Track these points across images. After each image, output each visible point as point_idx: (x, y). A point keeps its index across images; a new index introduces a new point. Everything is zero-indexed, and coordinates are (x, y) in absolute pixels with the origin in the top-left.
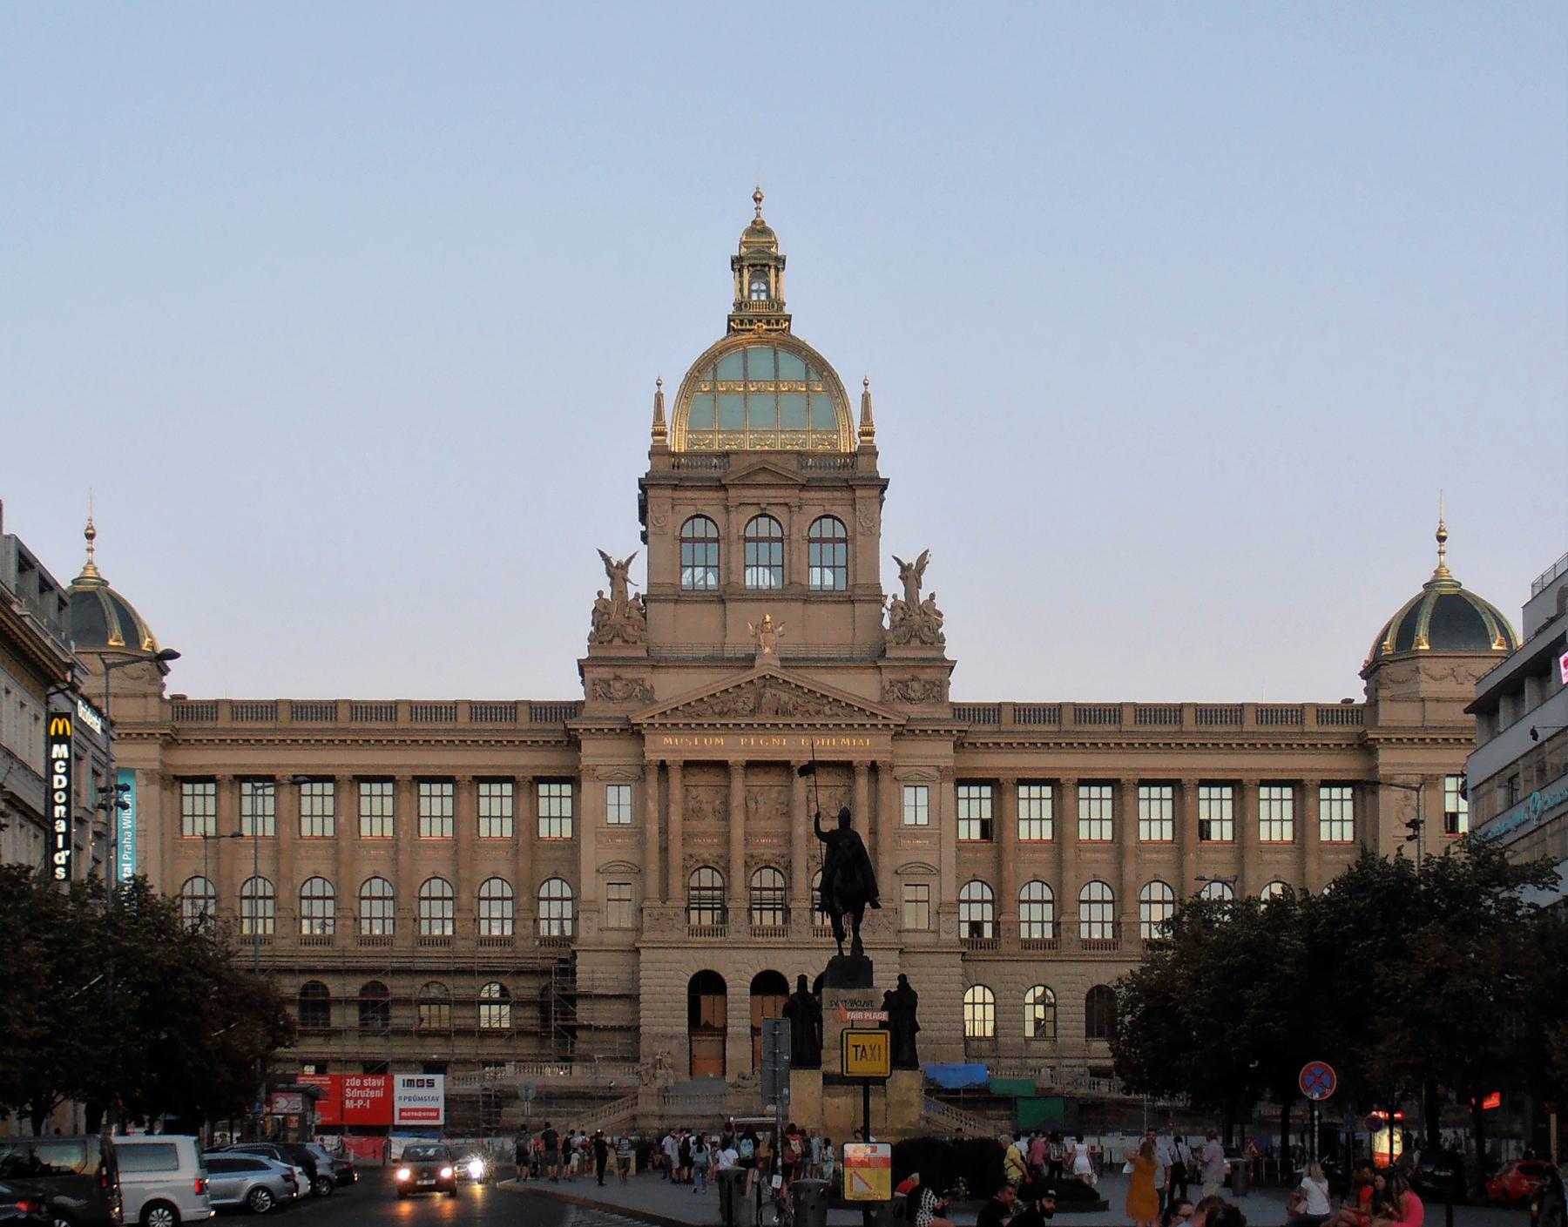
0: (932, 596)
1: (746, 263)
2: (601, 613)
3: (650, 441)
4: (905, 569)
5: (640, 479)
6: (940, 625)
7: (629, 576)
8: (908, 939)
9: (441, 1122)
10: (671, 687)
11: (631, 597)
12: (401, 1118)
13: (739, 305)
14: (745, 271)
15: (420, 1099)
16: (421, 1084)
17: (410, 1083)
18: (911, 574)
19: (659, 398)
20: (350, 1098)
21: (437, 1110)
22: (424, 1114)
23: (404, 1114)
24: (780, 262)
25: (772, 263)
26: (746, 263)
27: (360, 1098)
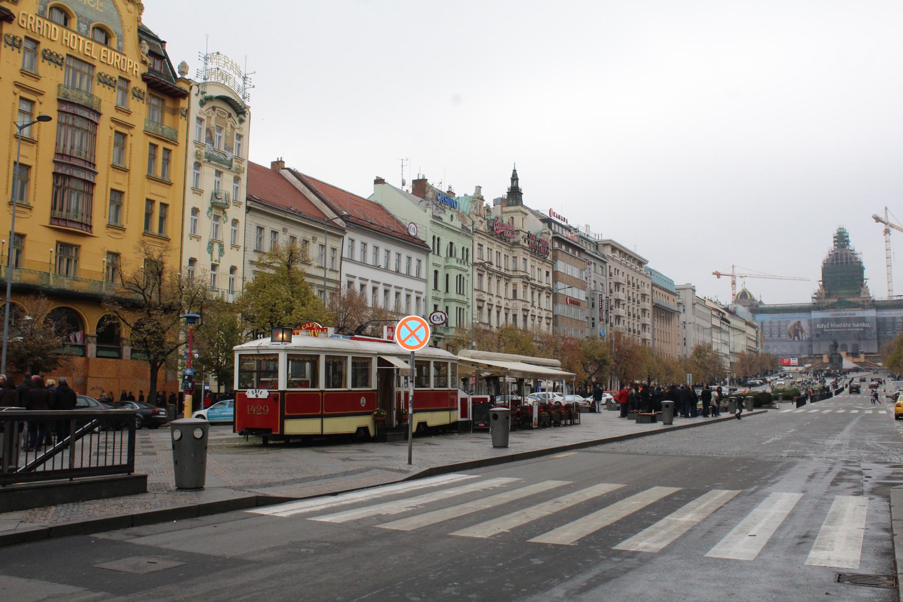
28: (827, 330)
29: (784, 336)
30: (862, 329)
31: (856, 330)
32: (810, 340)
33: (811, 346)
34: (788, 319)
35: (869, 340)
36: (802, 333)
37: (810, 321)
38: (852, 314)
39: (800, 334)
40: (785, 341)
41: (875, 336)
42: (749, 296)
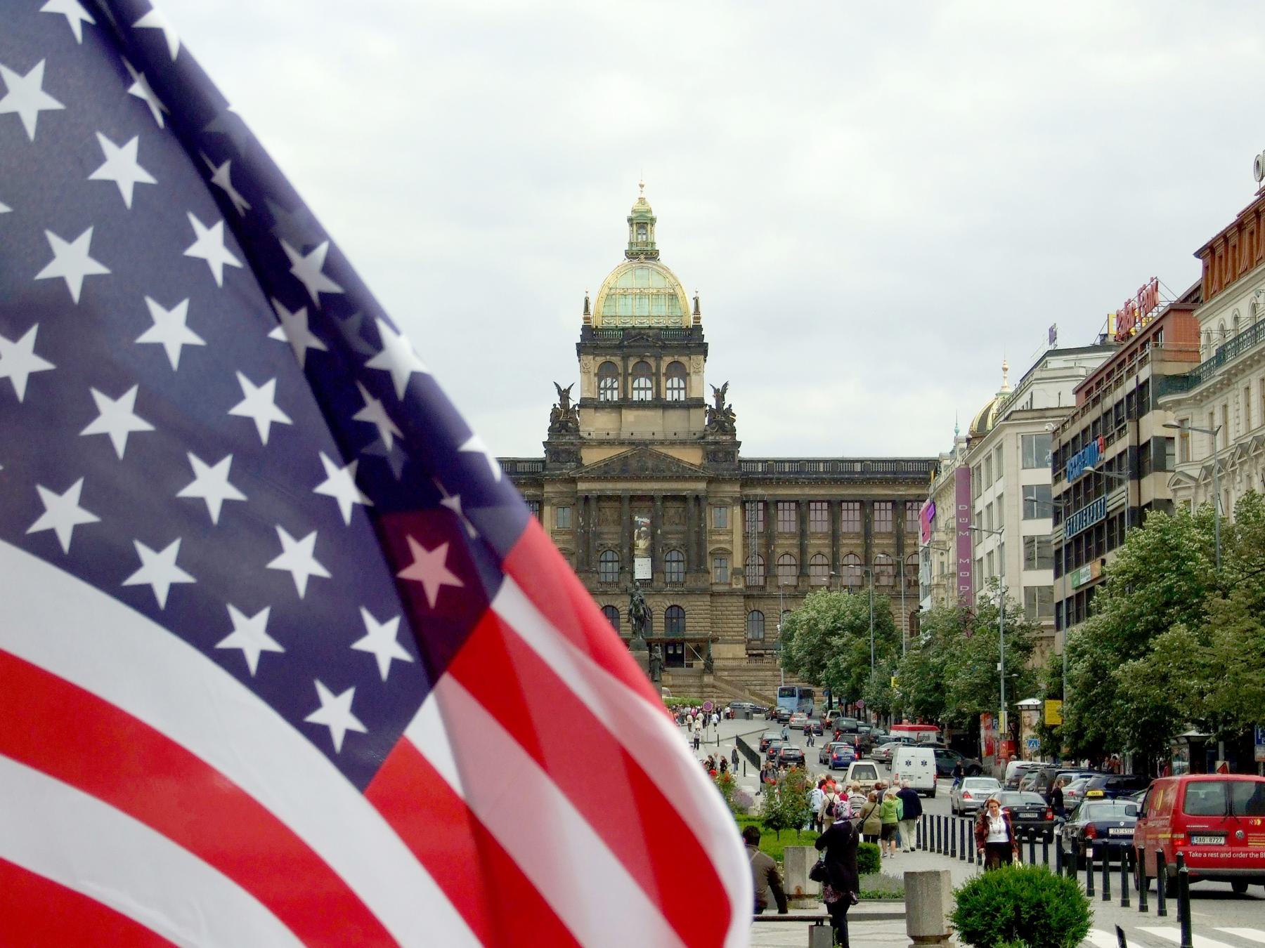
0: (730, 406)
1: (635, 222)
2: (555, 415)
3: (583, 323)
4: (716, 391)
5: (577, 344)
6: (735, 421)
7: (570, 396)
8: (715, 588)
10: (591, 457)
11: (571, 407)
13: (631, 244)
14: (635, 226)
18: (720, 395)
19: (587, 302)
24: (653, 220)
25: (648, 222)
26: (635, 222)
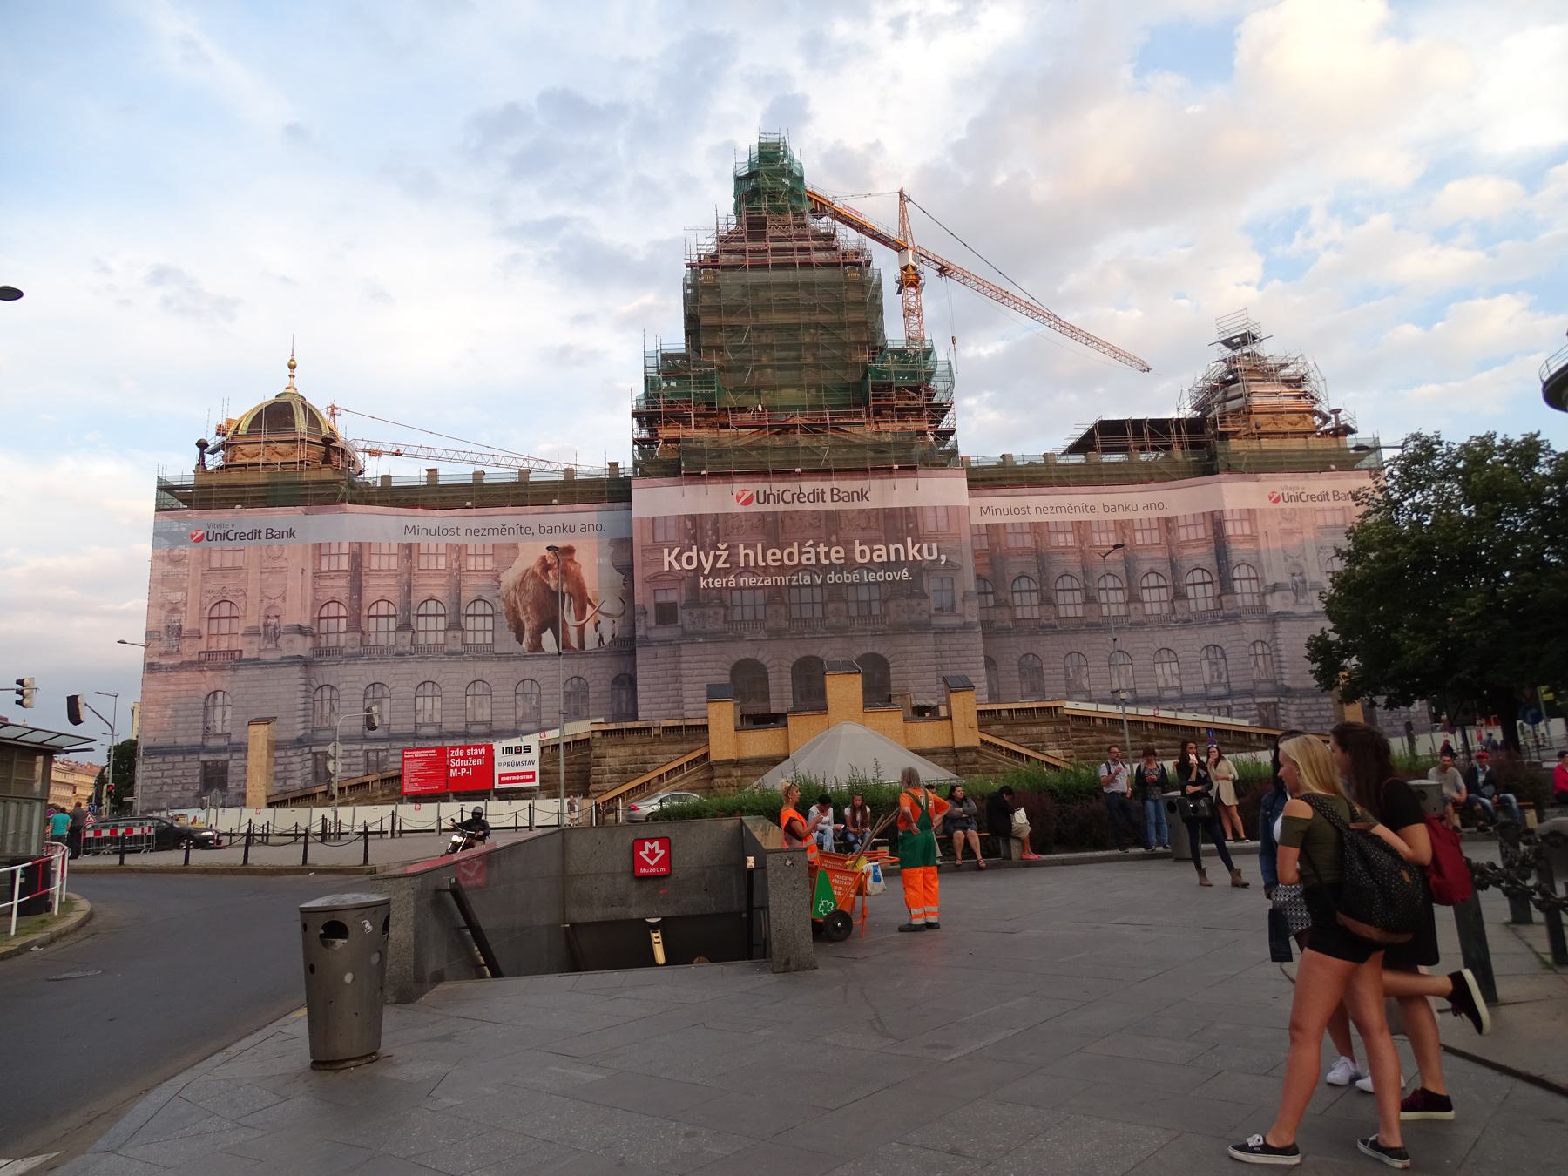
9: (537, 783)
12: (501, 782)
15: (518, 764)
16: (518, 750)
17: (509, 750)
20: (454, 768)
21: (533, 773)
22: (522, 777)
23: (503, 779)
27: (463, 767)
28: (718, 582)
29: (480, 630)
30: (905, 575)
31: (872, 577)
32: (625, 647)
33: (626, 682)
34: (509, 539)
35: (944, 631)
36: (581, 613)
37: (624, 545)
38: (850, 497)
39: (570, 618)
40: (486, 653)
41: (972, 613)
42: (301, 425)
